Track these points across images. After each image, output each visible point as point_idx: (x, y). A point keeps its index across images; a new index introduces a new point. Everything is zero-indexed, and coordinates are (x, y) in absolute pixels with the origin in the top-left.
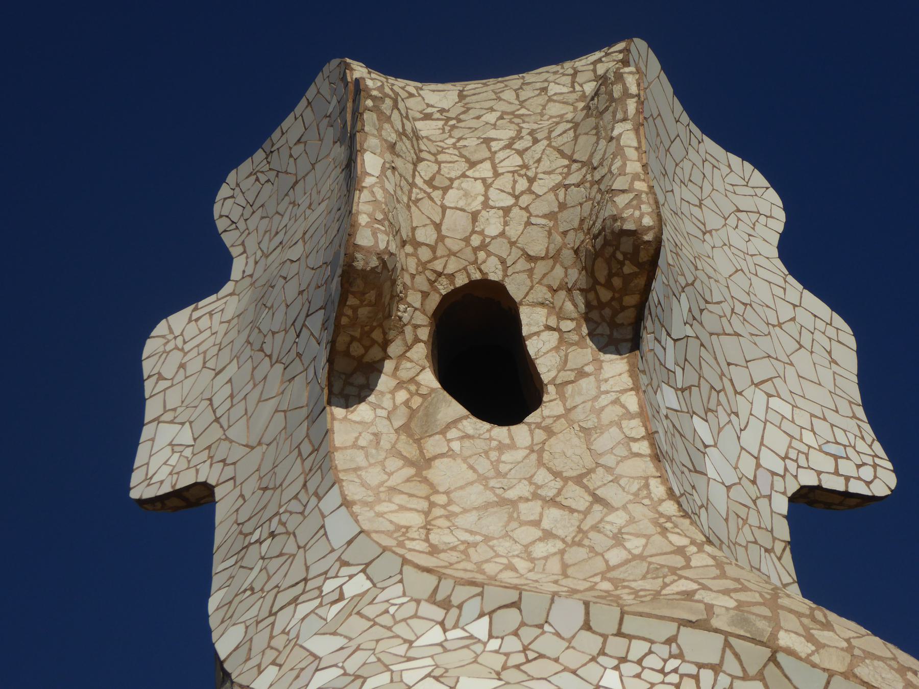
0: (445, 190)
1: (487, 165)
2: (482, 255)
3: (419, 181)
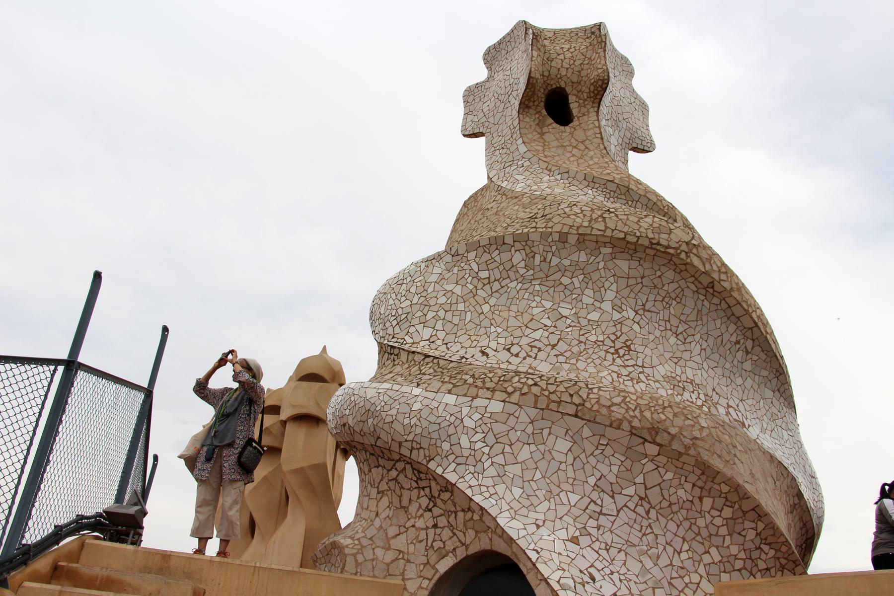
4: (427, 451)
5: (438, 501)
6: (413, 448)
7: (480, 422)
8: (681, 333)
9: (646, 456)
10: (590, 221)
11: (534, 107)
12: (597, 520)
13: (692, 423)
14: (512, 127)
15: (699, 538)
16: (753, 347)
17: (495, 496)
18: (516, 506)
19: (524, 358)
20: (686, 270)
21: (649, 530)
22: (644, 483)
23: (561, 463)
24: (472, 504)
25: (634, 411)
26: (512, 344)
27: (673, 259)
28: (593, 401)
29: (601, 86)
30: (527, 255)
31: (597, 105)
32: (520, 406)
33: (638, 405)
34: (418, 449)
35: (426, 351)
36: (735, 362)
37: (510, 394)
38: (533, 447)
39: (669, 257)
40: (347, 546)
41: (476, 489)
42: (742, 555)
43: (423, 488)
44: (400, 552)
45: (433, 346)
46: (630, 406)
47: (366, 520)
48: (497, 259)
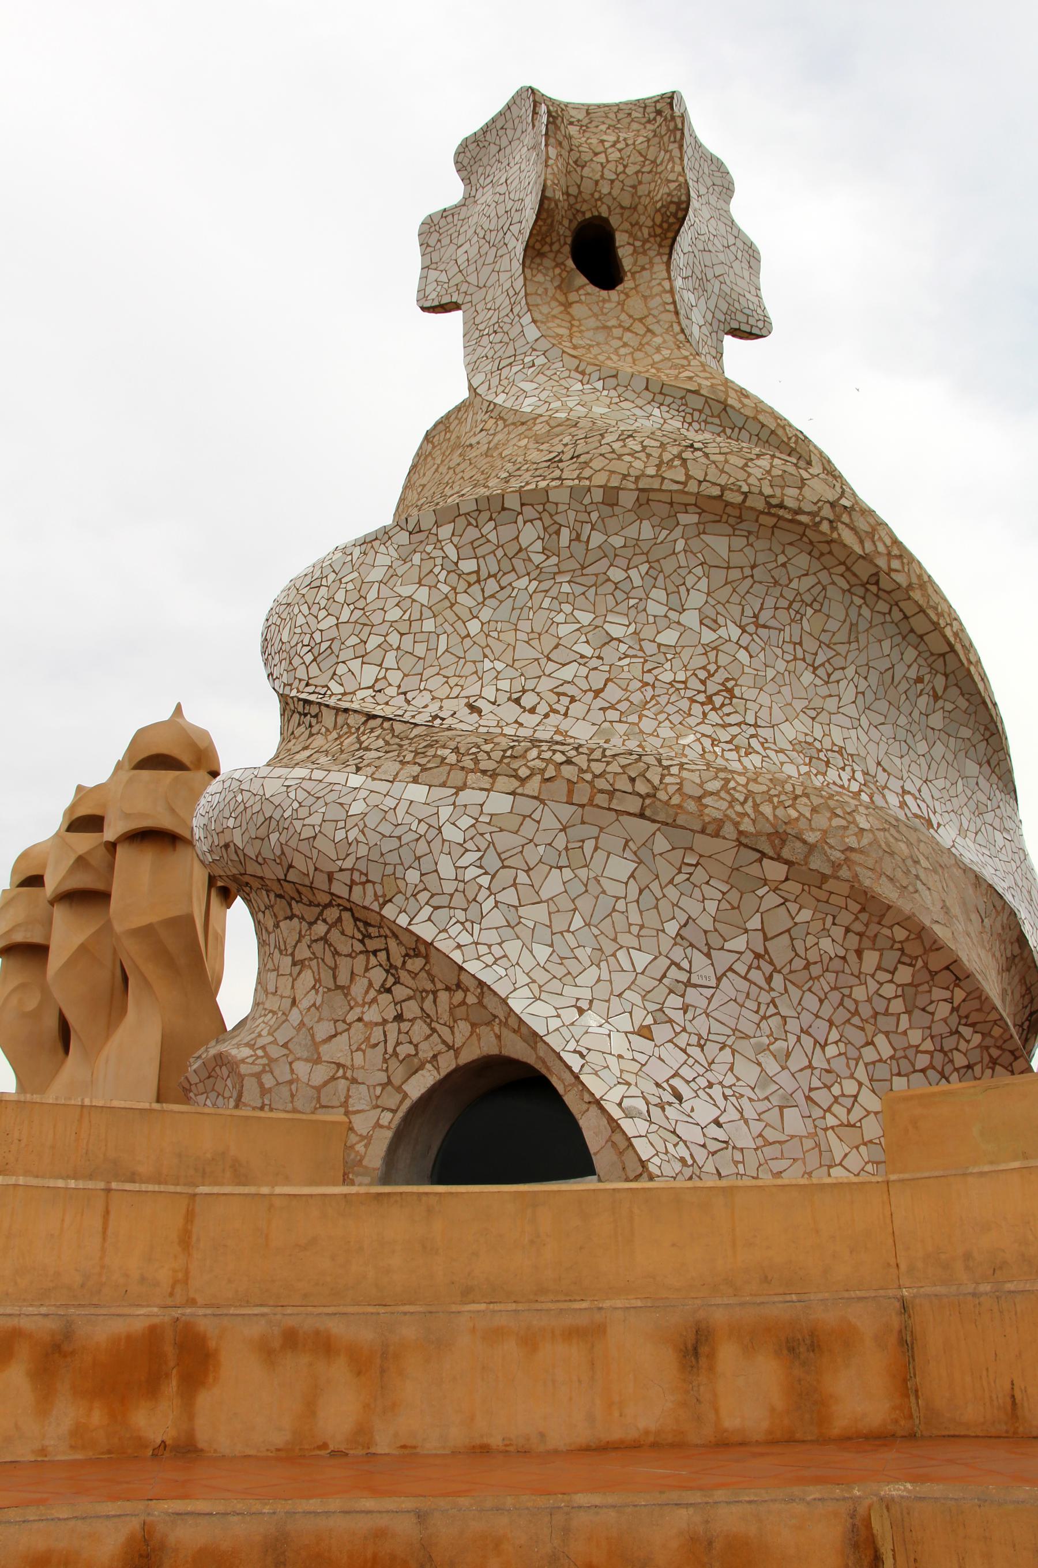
0: (583, 167)
1: (603, 155)
2: (599, 203)
3: (571, 162)
4: (378, 887)
5: (403, 974)
6: (353, 882)
7: (472, 832)
8: (823, 664)
9: (765, 882)
10: (659, 466)
11: (551, 255)
12: (683, 996)
13: (844, 823)
14: (511, 293)
15: (856, 1020)
16: (945, 688)
17: (503, 962)
18: (541, 976)
19: (546, 716)
20: (830, 552)
21: (772, 1010)
22: (763, 930)
23: (618, 898)
24: (463, 977)
25: (742, 804)
26: (524, 691)
27: (808, 532)
28: (672, 789)
29: (675, 215)
30: (545, 529)
31: (667, 250)
32: (542, 802)
33: (750, 794)
34: (363, 884)
35: (369, 707)
36: (916, 714)
37: (523, 781)
38: (567, 873)
39: (800, 530)
40: (243, 1061)
41: (470, 951)
42: (928, 1045)
43: (375, 953)
44: (339, 1065)
45: (380, 698)
46: (737, 795)
47: (274, 1013)
48: (493, 537)
